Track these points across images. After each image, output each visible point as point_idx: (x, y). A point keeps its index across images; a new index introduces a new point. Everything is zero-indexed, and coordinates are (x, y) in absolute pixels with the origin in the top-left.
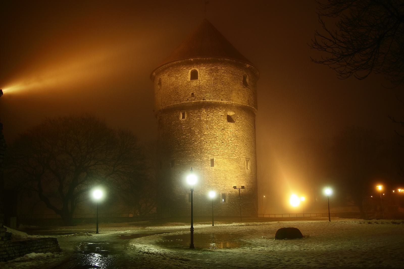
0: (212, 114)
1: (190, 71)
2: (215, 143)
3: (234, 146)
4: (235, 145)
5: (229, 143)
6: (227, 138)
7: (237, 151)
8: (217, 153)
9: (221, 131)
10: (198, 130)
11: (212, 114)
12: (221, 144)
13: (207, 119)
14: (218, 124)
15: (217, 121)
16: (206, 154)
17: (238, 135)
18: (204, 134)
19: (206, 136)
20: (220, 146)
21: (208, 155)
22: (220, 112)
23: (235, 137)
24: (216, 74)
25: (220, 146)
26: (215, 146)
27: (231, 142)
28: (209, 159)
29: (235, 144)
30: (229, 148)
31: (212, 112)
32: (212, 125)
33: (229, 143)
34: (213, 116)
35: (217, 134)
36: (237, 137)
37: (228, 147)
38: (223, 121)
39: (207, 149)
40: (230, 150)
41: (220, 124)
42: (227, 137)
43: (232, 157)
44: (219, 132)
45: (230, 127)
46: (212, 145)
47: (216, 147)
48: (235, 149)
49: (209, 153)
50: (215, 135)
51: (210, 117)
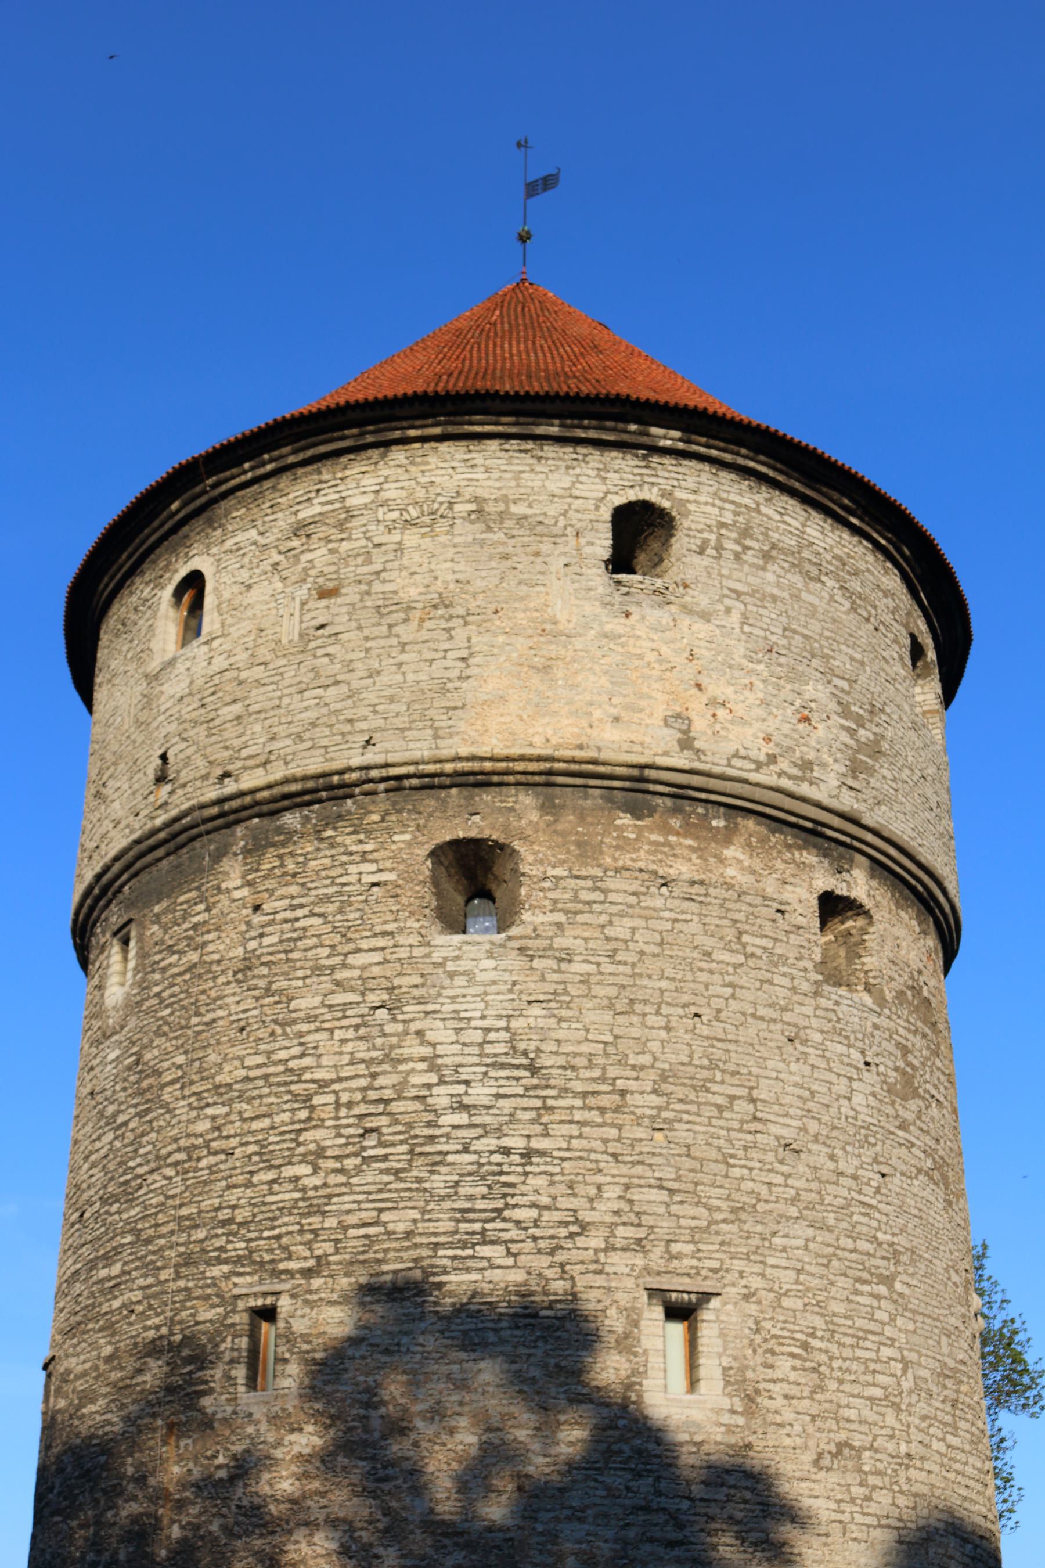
0: (294, 890)
1: (167, 593)
2: (301, 1150)
3: (497, 1158)
4: (507, 1151)
5: (432, 1139)
6: (413, 1092)
7: (533, 1205)
8: (309, 1244)
9: (357, 1027)
10: (180, 1059)
11: (294, 890)
12: (356, 1155)
13: (252, 945)
14: (333, 969)
15: (333, 947)
16: (216, 1271)
17: (549, 1046)
18: (218, 1079)
19: (229, 1103)
20: (342, 1179)
21: (227, 1277)
22: (364, 857)
23: (503, 1066)
24: (332, 551)
25: (342, 1179)
26: (297, 1179)
27: (462, 1118)
28: (236, 1318)
29: (507, 1142)
30: (438, 1183)
31: (294, 875)
32: (280, 992)
33: (432, 1139)
34: (302, 906)
35: (325, 1061)
36: (533, 1069)
37: (419, 1180)
38: (384, 934)
39: (224, 1223)
40: (448, 1204)
41: (352, 967)
42: (415, 1080)
43: (468, 1270)
44: (343, 1041)
45: (460, 981)
46: (271, 1175)
47: (304, 1190)
48: (512, 1185)
49: (239, 1260)
50: (307, 1076)
51: (271, 923)
